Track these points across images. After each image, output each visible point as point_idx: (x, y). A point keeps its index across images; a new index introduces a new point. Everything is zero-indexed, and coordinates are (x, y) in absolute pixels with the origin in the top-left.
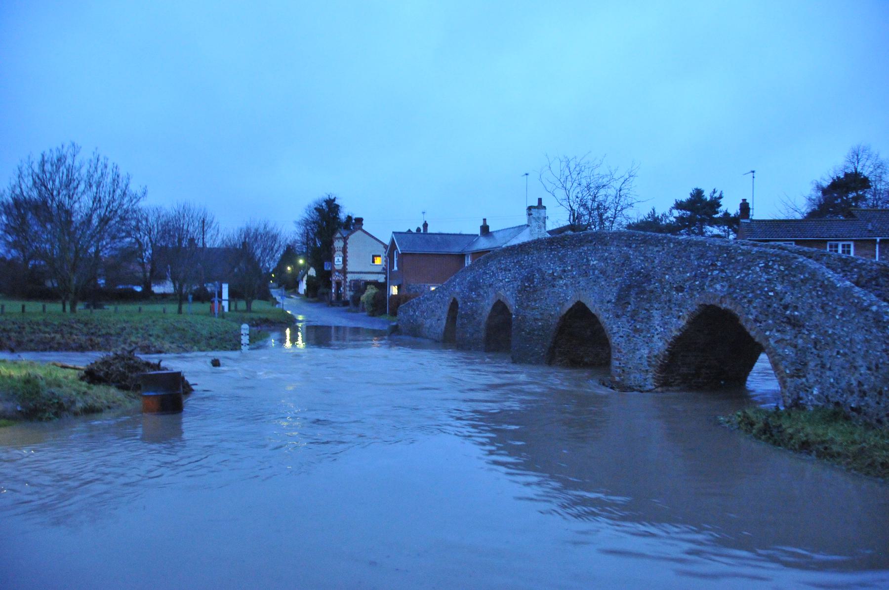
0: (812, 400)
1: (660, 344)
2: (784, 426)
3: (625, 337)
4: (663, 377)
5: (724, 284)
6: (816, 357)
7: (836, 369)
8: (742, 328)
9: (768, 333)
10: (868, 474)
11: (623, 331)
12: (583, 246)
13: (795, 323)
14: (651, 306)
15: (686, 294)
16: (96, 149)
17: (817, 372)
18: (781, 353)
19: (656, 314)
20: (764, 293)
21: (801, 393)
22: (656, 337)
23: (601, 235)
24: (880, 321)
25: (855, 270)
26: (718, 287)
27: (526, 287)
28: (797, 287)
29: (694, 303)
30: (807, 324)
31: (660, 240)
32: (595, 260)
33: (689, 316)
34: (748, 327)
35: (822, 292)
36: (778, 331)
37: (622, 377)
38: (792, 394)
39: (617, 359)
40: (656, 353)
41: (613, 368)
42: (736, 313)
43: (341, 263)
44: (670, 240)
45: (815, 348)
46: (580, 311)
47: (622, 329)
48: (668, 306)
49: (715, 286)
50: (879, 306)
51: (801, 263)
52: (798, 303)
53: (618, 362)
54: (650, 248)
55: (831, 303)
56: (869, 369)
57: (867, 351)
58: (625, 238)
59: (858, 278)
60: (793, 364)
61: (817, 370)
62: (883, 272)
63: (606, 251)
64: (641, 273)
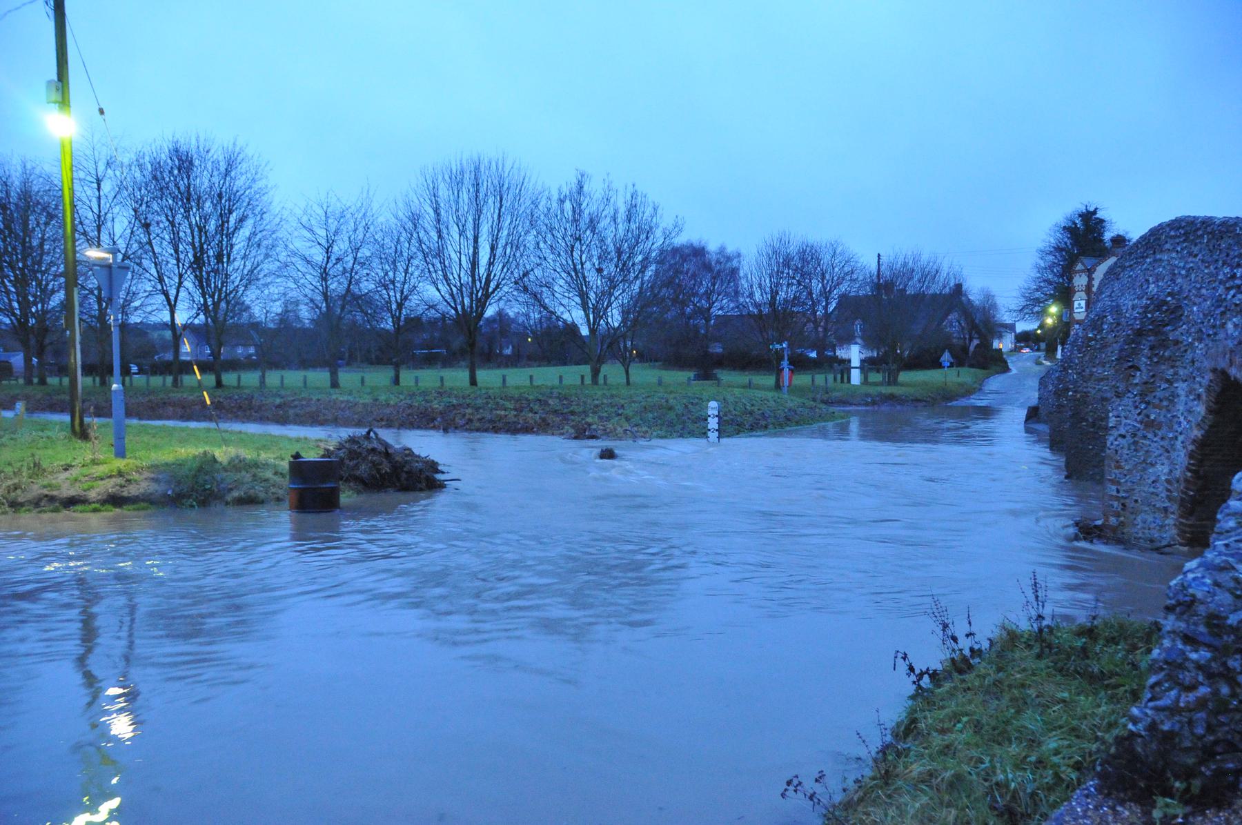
3: (1128, 437)
4: (1190, 526)
11: (1125, 425)
16: (608, 174)
27: (1091, 339)
37: (1122, 519)
39: (1113, 482)
43: (1083, 310)
47: (1124, 421)
53: (1114, 488)
64: (1166, 303)
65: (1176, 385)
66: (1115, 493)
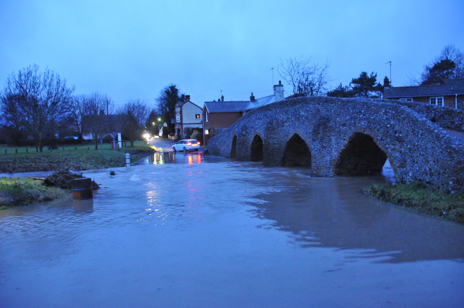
0: (408, 179)
1: (336, 154)
2: (391, 192)
3: (318, 151)
4: (338, 170)
5: (366, 121)
6: (410, 157)
7: (419, 162)
8: (375, 144)
9: (387, 146)
10: (428, 213)
12: (296, 105)
13: (400, 140)
14: (330, 134)
15: (347, 127)
17: (411, 165)
18: (395, 156)
19: (333, 138)
20: (385, 125)
21: (404, 175)
22: (334, 150)
23: (305, 99)
24: (439, 137)
25: (433, 111)
26: (363, 123)
27: (269, 127)
28: (401, 122)
29: (351, 132)
30: (406, 140)
31: (334, 100)
32: (303, 112)
33: (349, 139)
34: (378, 143)
35: (412, 124)
36: (392, 145)
37: (317, 171)
38: (399, 176)
39: (314, 162)
40: (334, 158)
41: (312, 167)
42: (372, 136)
43: (180, 119)
44: (339, 100)
45: (410, 152)
46: (297, 139)
47: (316, 147)
48: (339, 134)
49: (361, 123)
50: (438, 130)
51: (403, 109)
52: (402, 130)
54: (330, 104)
55: (416, 129)
56: (434, 162)
57: (433, 153)
58: (317, 100)
59: (434, 116)
60: (399, 161)
61: (411, 164)
62: (446, 112)
63: (308, 107)
64: (326, 117)
65: (331, 137)
66: (315, 165)
